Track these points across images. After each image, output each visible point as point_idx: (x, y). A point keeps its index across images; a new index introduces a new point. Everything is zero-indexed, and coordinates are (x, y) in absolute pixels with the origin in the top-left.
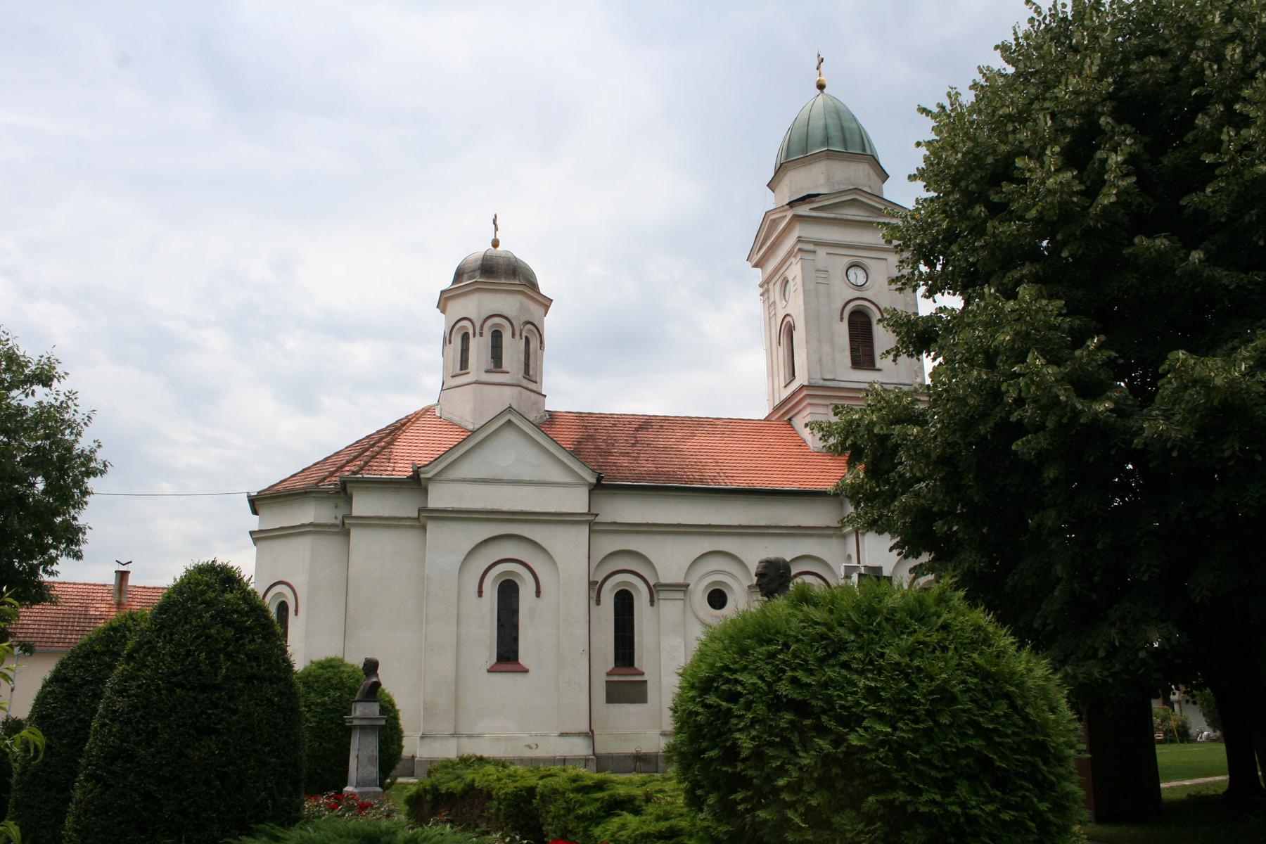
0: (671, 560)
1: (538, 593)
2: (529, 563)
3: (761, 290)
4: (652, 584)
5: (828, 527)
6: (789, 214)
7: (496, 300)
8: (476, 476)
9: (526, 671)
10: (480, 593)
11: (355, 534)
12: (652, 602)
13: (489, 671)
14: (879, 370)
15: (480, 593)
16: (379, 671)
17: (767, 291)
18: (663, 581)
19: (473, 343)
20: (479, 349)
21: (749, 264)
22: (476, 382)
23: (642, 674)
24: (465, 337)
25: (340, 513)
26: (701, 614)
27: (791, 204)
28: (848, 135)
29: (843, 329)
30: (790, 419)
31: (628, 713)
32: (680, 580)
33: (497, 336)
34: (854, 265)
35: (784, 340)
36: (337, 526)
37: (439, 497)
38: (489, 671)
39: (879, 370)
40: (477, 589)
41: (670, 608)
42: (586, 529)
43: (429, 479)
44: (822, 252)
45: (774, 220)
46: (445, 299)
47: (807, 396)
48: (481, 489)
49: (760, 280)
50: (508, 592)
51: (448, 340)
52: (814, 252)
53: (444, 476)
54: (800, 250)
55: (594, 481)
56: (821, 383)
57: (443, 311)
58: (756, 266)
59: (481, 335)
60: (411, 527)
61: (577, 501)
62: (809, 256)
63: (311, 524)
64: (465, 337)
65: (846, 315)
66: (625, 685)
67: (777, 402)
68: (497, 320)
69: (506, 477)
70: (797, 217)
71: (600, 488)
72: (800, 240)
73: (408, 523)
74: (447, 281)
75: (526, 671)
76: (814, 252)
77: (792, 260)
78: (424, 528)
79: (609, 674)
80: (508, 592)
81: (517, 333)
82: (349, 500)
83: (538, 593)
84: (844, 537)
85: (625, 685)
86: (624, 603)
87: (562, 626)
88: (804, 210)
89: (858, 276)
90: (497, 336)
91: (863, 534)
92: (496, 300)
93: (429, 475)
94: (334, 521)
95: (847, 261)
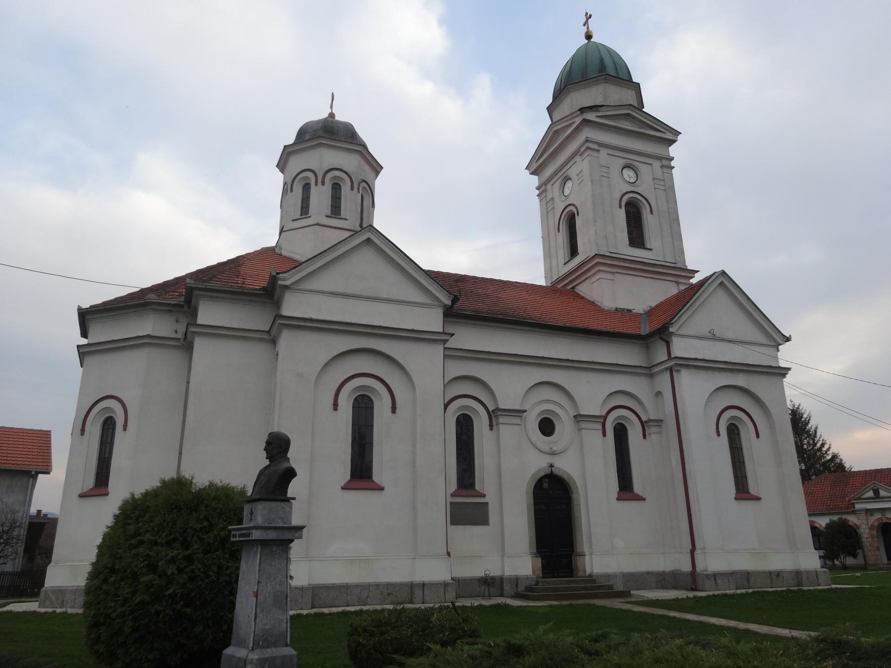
0: (510, 387)
1: (394, 409)
2: (385, 380)
3: (537, 192)
4: (491, 409)
5: (640, 367)
6: (578, 120)
7: (329, 162)
8: (333, 289)
9: (382, 489)
10: (335, 406)
11: (200, 345)
12: (491, 426)
13: (343, 488)
14: (650, 250)
15: (335, 406)
16: (289, 455)
17: (545, 191)
18: (501, 407)
19: (314, 191)
20: (320, 197)
21: (527, 172)
22: (318, 224)
23: (484, 496)
24: (307, 188)
25: (182, 329)
26: (534, 440)
27: (582, 110)
28: (618, 68)
29: (622, 214)
30: (573, 288)
31: (469, 536)
32: (518, 408)
33: (336, 188)
34: (627, 166)
35: (564, 227)
36: (179, 339)
37: (293, 306)
38: (343, 488)
39: (650, 250)
40: (332, 402)
41: (508, 431)
42: (439, 350)
43: (286, 287)
44: (604, 152)
45: (556, 132)
46: (288, 153)
47: (598, 263)
48: (339, 301)
49: (537, 184)
50: (363, 408)
51: (287, 189)
52: (599, 151)
53: (303, 286)
54: (588, 148)
55: (449, 303)
56: (608, 254)
57: (282, 171)
58: (533, 173)
59: (323, 183)
60: (261, 340)
61: (431, 320)
62: (594, 154)
63: (148, 336)
64: (307, 188)
65: (623, 204)
66: (468, 507)
67: (555, 278)
68: (337, 173)
69: (365, 294)
70: (586, 122)
71: (450, 314)
72: (587, 141)
73: (258, 336)
74: (291, 140)
75: (382, 489)
76: (599, 151)
77: (578, 158)
78: (274, 342)
79: (453, 495)
80: (363, 408)
81: (356, 187)
82: (194, 314)
83: (394, 409)
84: (651, 376)
85: (468, 509)
86: (465, 425)
87: (415, 445)
88: (591, 116)
89: (629, 174)
90: (336, 188)
91: (678, 371)
92: (329, 162)
93: (288, 283)
94: (173, 335)
95: (622, 162)
